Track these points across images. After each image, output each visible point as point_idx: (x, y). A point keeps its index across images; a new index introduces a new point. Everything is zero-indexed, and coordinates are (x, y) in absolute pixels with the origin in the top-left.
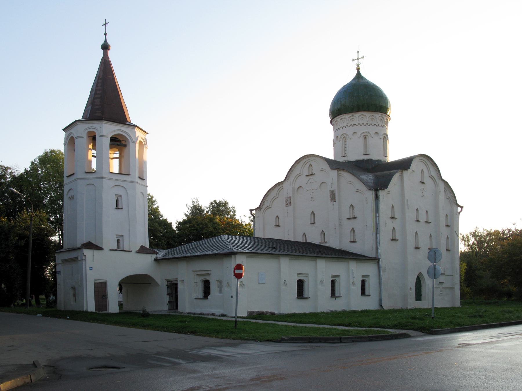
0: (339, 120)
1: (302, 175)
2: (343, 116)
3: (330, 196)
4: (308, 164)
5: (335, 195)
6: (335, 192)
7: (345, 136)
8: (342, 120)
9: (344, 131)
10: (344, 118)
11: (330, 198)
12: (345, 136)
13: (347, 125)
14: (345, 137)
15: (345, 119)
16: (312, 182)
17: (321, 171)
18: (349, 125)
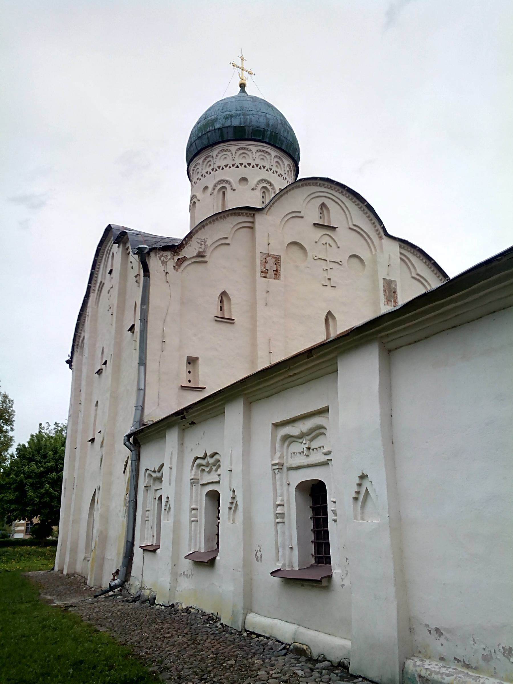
0: (254, 149)
1: (302, 217)
2: (268, 148)
3: (385, 292)
4: (319, 202)
5: (394, 292)
6: (396, 285)
7: (267, 186)
8: (260, 153)
9: (264, 174)
10: (266, 152)
11: (384, 295)
12: (267, 186)
13: (271, 167)
14: (264, 187)
15: (268, 157)
16: (329, 244)
17: (350, 228)
18: (274, 169)
